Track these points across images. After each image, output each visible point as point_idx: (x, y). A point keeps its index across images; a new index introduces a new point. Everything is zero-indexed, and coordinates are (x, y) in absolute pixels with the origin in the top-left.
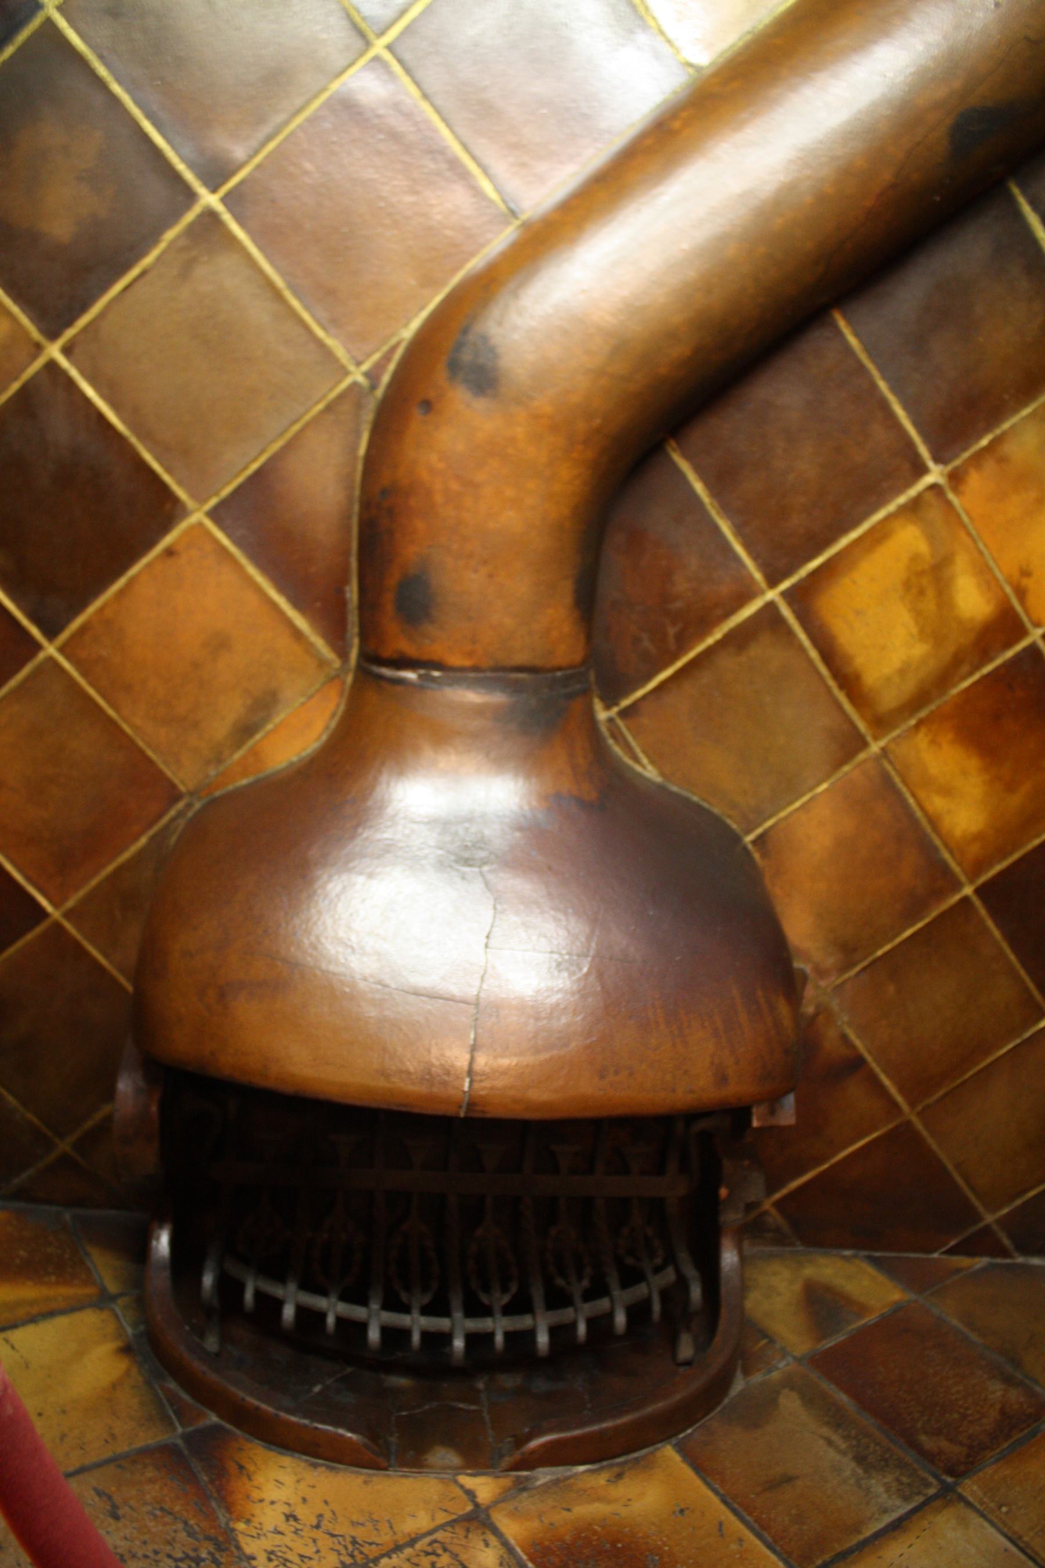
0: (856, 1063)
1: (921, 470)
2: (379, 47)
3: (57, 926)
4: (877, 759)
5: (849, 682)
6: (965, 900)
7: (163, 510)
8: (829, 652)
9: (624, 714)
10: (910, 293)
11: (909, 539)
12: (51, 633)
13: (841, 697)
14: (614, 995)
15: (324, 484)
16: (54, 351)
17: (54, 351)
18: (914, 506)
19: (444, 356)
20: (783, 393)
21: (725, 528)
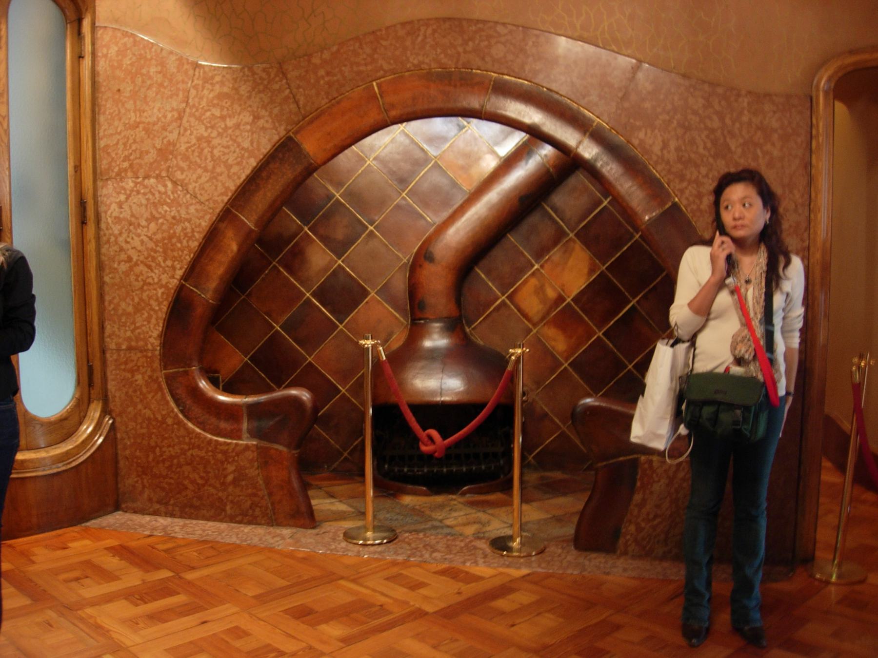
0: (546, 415)
1: (533, 266)
2: (404, 194)
3: (344, 394)
4: (535, 334)
5: (526, 316)
6: (565, 368)
7: (366, 293)
8: (519, 310)
9: (473, 329)
10: (524, 227)
11: (533, 281)
12: (341, 323)
13: (524, 320)
14: (468, 380)
15: (400, 285)
16: (340, 262)
17: (340, 262)
18: (533, 274)
19: (424, 255)
20: (498, 254)
21: (490, 284)
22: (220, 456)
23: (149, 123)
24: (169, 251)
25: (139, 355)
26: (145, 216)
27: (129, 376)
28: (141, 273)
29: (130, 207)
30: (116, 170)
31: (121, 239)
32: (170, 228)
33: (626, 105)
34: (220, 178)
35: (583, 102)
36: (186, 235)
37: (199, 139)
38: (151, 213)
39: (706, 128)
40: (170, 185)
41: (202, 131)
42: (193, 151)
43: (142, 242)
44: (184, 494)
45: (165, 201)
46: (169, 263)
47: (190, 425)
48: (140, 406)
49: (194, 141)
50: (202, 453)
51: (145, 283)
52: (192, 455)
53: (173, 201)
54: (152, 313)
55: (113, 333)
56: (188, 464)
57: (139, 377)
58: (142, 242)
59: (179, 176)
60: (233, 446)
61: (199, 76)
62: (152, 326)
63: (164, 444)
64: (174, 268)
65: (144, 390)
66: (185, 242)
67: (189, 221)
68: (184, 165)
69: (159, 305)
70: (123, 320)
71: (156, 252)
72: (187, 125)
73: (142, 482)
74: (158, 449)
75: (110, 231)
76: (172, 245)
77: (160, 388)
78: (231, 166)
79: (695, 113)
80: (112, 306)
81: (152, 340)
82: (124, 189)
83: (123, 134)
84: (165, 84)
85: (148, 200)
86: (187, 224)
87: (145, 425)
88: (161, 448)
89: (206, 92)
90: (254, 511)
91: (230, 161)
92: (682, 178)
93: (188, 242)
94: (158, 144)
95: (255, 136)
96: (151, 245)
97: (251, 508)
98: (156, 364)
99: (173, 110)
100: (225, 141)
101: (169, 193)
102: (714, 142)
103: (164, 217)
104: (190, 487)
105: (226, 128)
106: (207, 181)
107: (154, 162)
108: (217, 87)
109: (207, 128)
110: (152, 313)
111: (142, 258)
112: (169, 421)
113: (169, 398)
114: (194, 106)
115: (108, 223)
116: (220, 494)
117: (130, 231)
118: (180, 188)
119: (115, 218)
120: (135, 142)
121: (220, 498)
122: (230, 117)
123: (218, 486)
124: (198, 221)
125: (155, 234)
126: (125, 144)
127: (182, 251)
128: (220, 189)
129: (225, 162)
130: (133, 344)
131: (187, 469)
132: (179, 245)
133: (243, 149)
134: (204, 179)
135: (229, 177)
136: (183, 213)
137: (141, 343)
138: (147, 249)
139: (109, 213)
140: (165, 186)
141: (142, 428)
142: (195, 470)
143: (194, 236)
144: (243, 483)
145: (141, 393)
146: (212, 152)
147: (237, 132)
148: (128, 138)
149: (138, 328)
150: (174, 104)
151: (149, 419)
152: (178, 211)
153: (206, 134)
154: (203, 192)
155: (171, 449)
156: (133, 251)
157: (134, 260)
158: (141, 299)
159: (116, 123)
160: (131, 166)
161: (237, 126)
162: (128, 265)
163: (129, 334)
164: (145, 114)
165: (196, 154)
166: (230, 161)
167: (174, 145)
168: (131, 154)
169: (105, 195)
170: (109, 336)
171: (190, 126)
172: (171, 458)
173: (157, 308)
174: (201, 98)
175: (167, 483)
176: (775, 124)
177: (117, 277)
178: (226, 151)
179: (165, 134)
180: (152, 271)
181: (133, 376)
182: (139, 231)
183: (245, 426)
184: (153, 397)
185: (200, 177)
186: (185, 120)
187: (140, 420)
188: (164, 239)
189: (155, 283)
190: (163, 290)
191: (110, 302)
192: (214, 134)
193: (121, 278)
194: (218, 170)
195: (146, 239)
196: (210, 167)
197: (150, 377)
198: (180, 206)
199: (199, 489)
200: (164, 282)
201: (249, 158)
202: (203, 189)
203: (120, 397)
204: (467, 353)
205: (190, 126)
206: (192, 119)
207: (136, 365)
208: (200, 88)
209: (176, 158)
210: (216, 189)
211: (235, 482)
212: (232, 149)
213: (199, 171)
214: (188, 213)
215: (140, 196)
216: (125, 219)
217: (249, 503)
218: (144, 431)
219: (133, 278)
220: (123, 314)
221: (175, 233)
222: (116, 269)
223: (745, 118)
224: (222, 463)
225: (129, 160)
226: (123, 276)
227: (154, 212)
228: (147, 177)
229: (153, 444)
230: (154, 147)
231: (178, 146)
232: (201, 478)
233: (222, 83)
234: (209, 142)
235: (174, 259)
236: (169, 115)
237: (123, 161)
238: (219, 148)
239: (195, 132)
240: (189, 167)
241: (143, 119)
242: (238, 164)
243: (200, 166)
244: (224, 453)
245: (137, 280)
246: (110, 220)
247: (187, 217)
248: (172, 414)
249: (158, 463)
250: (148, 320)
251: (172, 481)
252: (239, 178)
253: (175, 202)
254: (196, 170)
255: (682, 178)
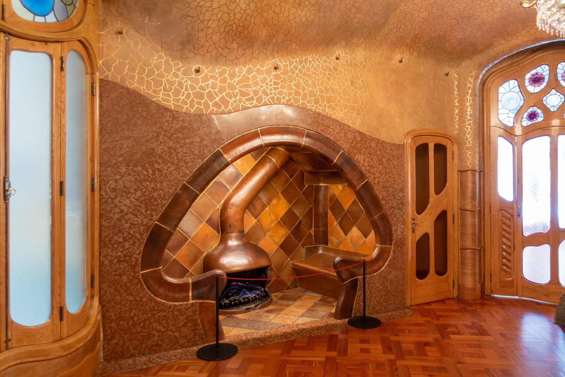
22: (176, 313)
23: (137, 138)
24: (149, 206)
25: (125, 265)
26: (133, 188)
27: (117, 278)
28: (130, 219)
29: (124, 182)
30: (114, 161)
31: (116, 201)
32: (150, 194)
33: (352, 145)
34: (181, 168)
35: (338, 143)
36: (160, 197)
37: (169, 148)
38: (138, 186)
39: (376, 154)
40: (150, 171)
41: (171, 144)
42: (166, 154)
43: (131, 202)
44: (152, 339)
45: (147, 179)
46: (149, 212)
47: (158, 299)
48: (124, 295)
49: (166, 149)
50: (165, 314)
51: (132, 224)
52: (159, 316)
53: (152, 179)
54: (136, 240)
55: (107, 255)
56: (155, 322)
57: (125, 278)
58: (131, 202)
59: (156, 166)
60: (184, 306)
61: (170, 116)
62: (136, 248)
63: (140, 313)
64: (152, 215)
65: (128, 285)
66: (159, 201)
67: (162, 190)
68: (159, 160)
69: (141, 236)
70: (116, 246)
71: (140, 207)
72: (162, 140)
73: (123, 340)
74: (136, 317)
75: (108, 196)
76: (151, 203)
77: (140, 282)
78: (188, 163)
79: (373, 149)
80: (108, 239)
81: (135, 256)
82: (120, 173)
83: (119, 142)
84: (149, 118)
85: (136, 179)
86: (161, 191)
87: (127, 305)
88: (138, 316)
89: (174, 125)
90: (195, 338)
91: (187, 160)
92: (369, 172)
93: (161, 201)
94: (144, 148)
95: (201, 148)
96: (137, 203)
97: (193, 336)
98: (139, 268)
99: (154, 132)
100: (184, 150)
101: (150, 175)
102: (379, 159)
103: (146, 188)
104: (157, 334)
105: (185, 144)
106: (174, 170)
107: (140, 159)
108: (181, 123)
109: (174, 143)
110: (136, 240)
111: (130, 210)
112: (145, 300)
113: (145, 286)
114: (166, 131)
115: (107, 192)
116: (176, 334)
117: (123, 196)
118: (157, 173)
119: (112, 188)
120: (128, 147)
121: (175, 336)
122: (188, 138)
123: (174, 329)
124: (168, 190)
125: (140, 197)
126: (121, 148)
127: (158, 206)
128: (181, 173)
129: (185, 161)
130: (122, 259)
131: (155, 324)
132: (156, 203)
133: (195, 154)
134: (172, 169)
135: (187, 168)
136: (159, 185)
137: (128, 258)
138: (134, 205)
139: (108, 185)
140: (148, 172)
141: (125, 307)
142: (160, 324)
143: (165, 198)
144: (190, 324)
145: (126, 287)
146: (177, 155)
147: (192, 146)
148: (123, 145)
149: (125, 250)
150: (154, 129)
151: (131, 301)
152: (156, 185)
153: (173, 146)
154: (171, 175)
155: (145, 315)
156: (125, 207)
157: (125, 212)
158: (129, 233)
159: (115, 135)
160: (124, 159)
161: (192, 143)
162: (120, 215)
163: (119, 254)
164: (135, 132)
165: (167, 155)
166: (187, 160)
167: (154, 150)
168: (125, 153)
169: (105, 176)
170: (105, 257)
171: (165, 141)
172: (145, 320)
173: (140, 237)
174: (171, 128)
175: (141, 336)
176: (396, 154)
177: (112, 222)
178: (185, 155)
179: (148, 144)
180: (137, 217)
181: (120, 278)
182: (129, 196)
183: (190, 294)
184: (134, 288)
185: (170, 167)
186: (161, 138)
187: (124, 302)
188: (146, 199)
189: (139, 224)
190: (144, 227)
191: (106, 237)
192: (179, 146)
193: (115, 223)
194: (180, 164)
195: (133, 200)
196: (176, 162)
197: (132, 277)
198: (157, 182)
199: (162, 334)
200: (145, 223)
201: (198, 159)
202: (172, 173)
203: (110, 292)
204: (250, 244)
205: (165, 141)
206: (165, 138)
207: (123, 271)
208: (170, 122)
209: (155, 157)
210: (179, 174)
211: (185, 325)
212: (189, 154)
213: (169, 164)
214: (161, 186)
215: (130, 176)
216: (119, 189)
217: (193, 334)
218: (126, 309)
219: (123, 222)
220: (115, 243)
221: (153, 196)
222: (111, 217)
223: (387, 152)
224: (177, 316)
225: (123, 157)
226: (117, 222)
227: (140, 185)
228: (136, 166)
229: (132, 315)
230: (141, 150)
231: (156, 150)
232: (164, 327)
233: (183, 121)
234: (175, 150)
235: (152, 210)
236: (151, 135)
237: (119, 157)
238: (181, 153)
239: (167, 144)
240: (163, 163)
241: (134, 135)
242: (192, 162)
243: (170, 162)
244: (179, 311)
245: (126, 223)
246: (108, 190)
247: (162, 188)
248: (146, 296)
249: (135, 325)
250: (133, 244)
251: (145, 334)
252: (193, 169)
253: (155, 180)
254: (166, 164)
255: (369, 172)
